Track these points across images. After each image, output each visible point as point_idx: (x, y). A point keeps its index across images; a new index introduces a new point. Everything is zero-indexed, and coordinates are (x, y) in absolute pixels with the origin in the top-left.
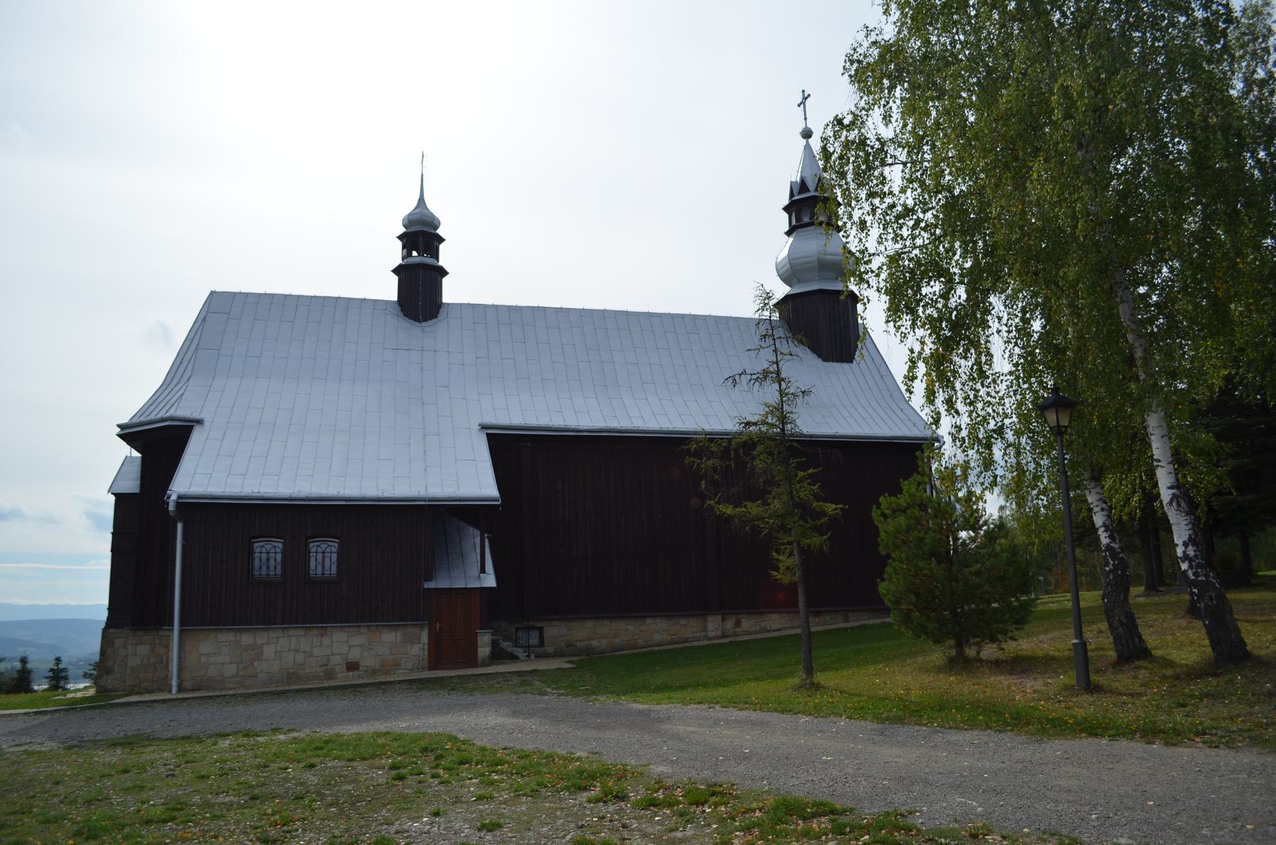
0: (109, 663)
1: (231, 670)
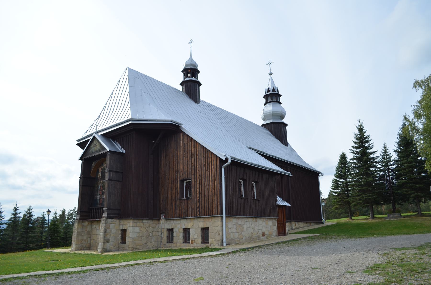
0: (108, 237)
1: (237, 235)
